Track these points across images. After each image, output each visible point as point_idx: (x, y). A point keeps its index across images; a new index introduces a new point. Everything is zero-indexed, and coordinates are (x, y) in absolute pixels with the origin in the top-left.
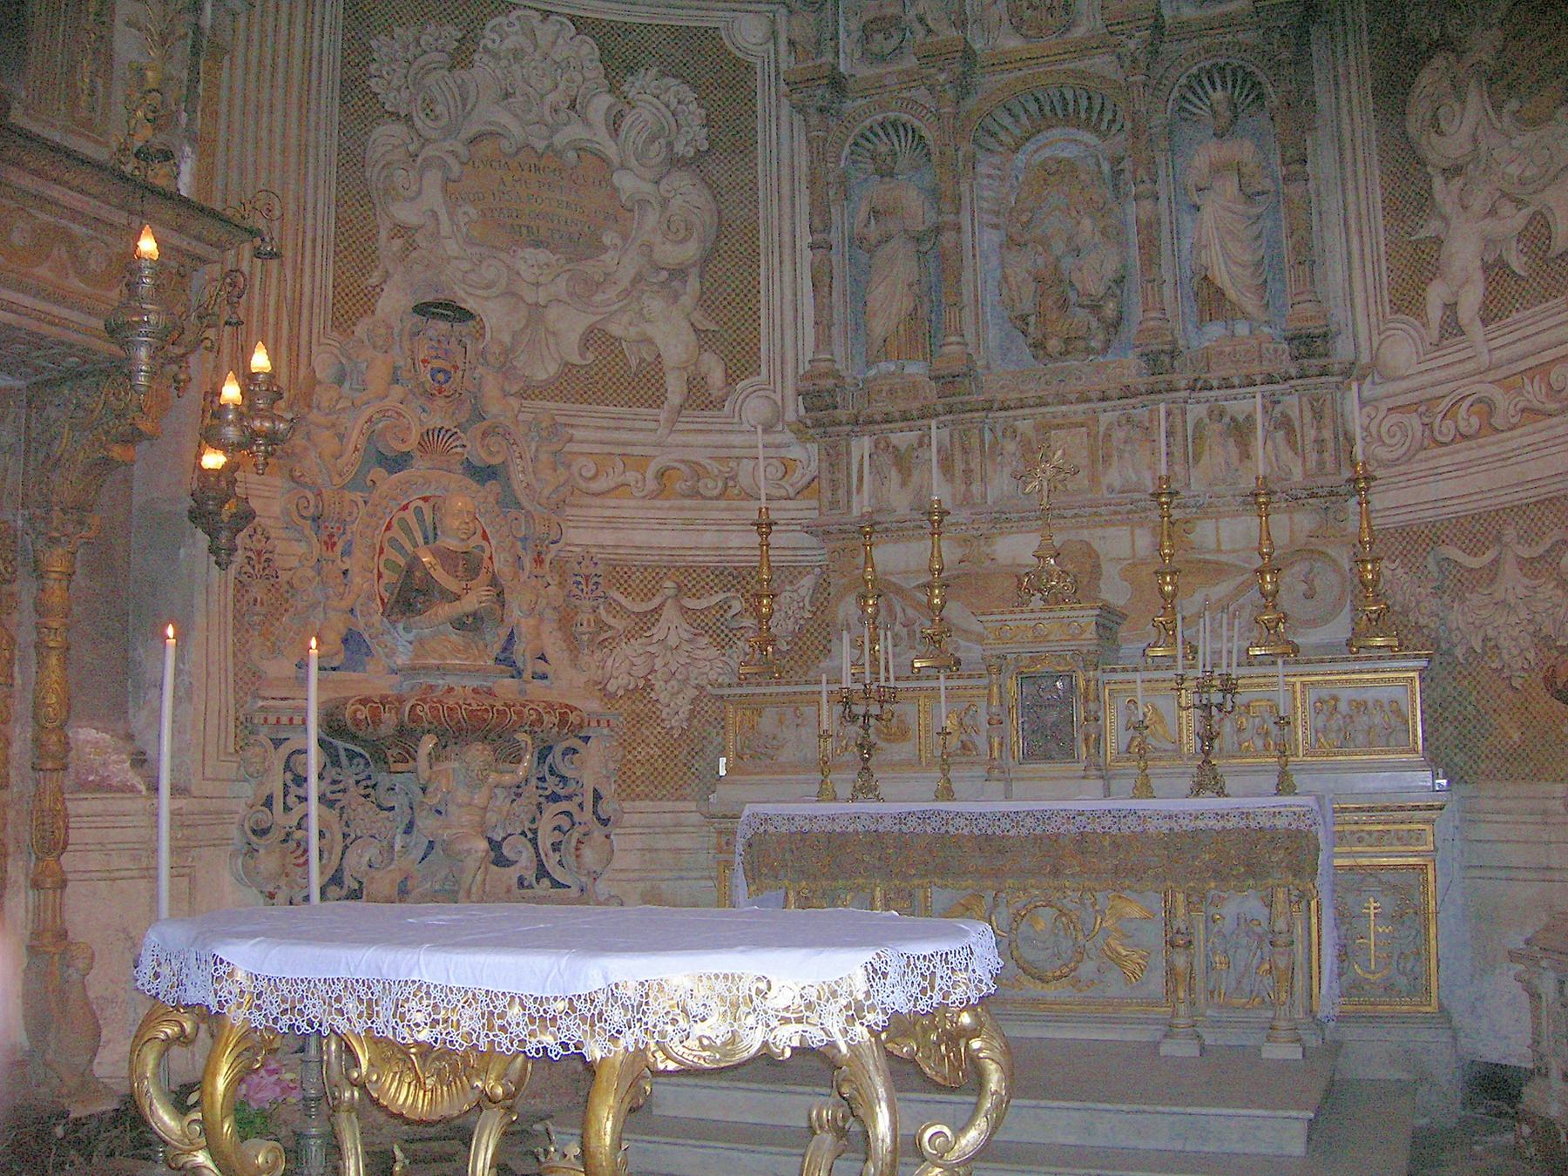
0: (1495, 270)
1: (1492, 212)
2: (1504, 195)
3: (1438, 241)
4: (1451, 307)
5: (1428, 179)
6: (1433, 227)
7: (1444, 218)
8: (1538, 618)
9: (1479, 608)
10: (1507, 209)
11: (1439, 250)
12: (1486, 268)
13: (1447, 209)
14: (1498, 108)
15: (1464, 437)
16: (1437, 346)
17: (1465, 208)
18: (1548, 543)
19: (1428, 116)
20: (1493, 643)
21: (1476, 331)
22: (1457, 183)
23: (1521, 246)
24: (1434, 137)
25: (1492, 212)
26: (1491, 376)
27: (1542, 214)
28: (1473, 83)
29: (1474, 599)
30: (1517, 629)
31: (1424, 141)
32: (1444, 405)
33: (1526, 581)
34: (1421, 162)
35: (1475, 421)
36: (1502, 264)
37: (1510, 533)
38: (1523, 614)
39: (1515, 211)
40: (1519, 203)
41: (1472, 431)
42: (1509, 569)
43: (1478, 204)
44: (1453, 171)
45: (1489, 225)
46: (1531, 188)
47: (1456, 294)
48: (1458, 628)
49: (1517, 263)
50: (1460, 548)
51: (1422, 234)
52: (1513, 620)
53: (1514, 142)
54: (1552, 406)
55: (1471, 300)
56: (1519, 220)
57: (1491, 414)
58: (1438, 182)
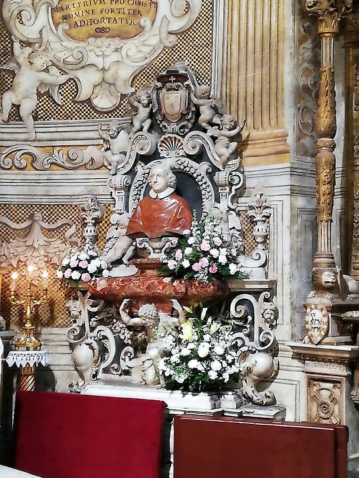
0: (44, 94)
1: (47, 70)
2: (54, 64)
3: (13, 74)
4: (17, 107)
5: (12, 42)
6: (12, 66)
7: (18, 64)
8: (50, 255)
9: (17, 247)
10: (54, 70)
11: (13, 78)
12: (39, 95)
13: (21, 60)
14: (57, 25)
15: (19, 169)
16: (7, 122)
17: (31, 63)
18: (59, 223)
19: (16, 12)
20: (23, 264)
21: (30, 121)
22: (28, 50)
23: (60, 91)
24: (18, 24)
25: (47, 70)
26: (36, 144)
27: (74, 81)
28: (44, 7)
29: (14, 242)
30: (38, 259)
31: (12, 23)
32: (7, 151)
33: (45, 238)
34: (10, 34)
35: (24, 163)
36: (48, 94)
37: (38, 216)
38: (42, 252)
39: (59, 74)
40: (63, 72)
41: (22, 166)
42: (37, 230)
43: (39, 62)
44: (26, 44)
45: (44, 76)
46: (70, 67)
47: (20, 101)
48: (4, 255)
49: (58, 99)
50: (9, 218)
51: (5, 67)
52: (35, 254)
53: (64, 44)
54: (67, 165)
55: (28, 106)
56: (63, 79)
57: (33, 161)
58: (17, 45)
